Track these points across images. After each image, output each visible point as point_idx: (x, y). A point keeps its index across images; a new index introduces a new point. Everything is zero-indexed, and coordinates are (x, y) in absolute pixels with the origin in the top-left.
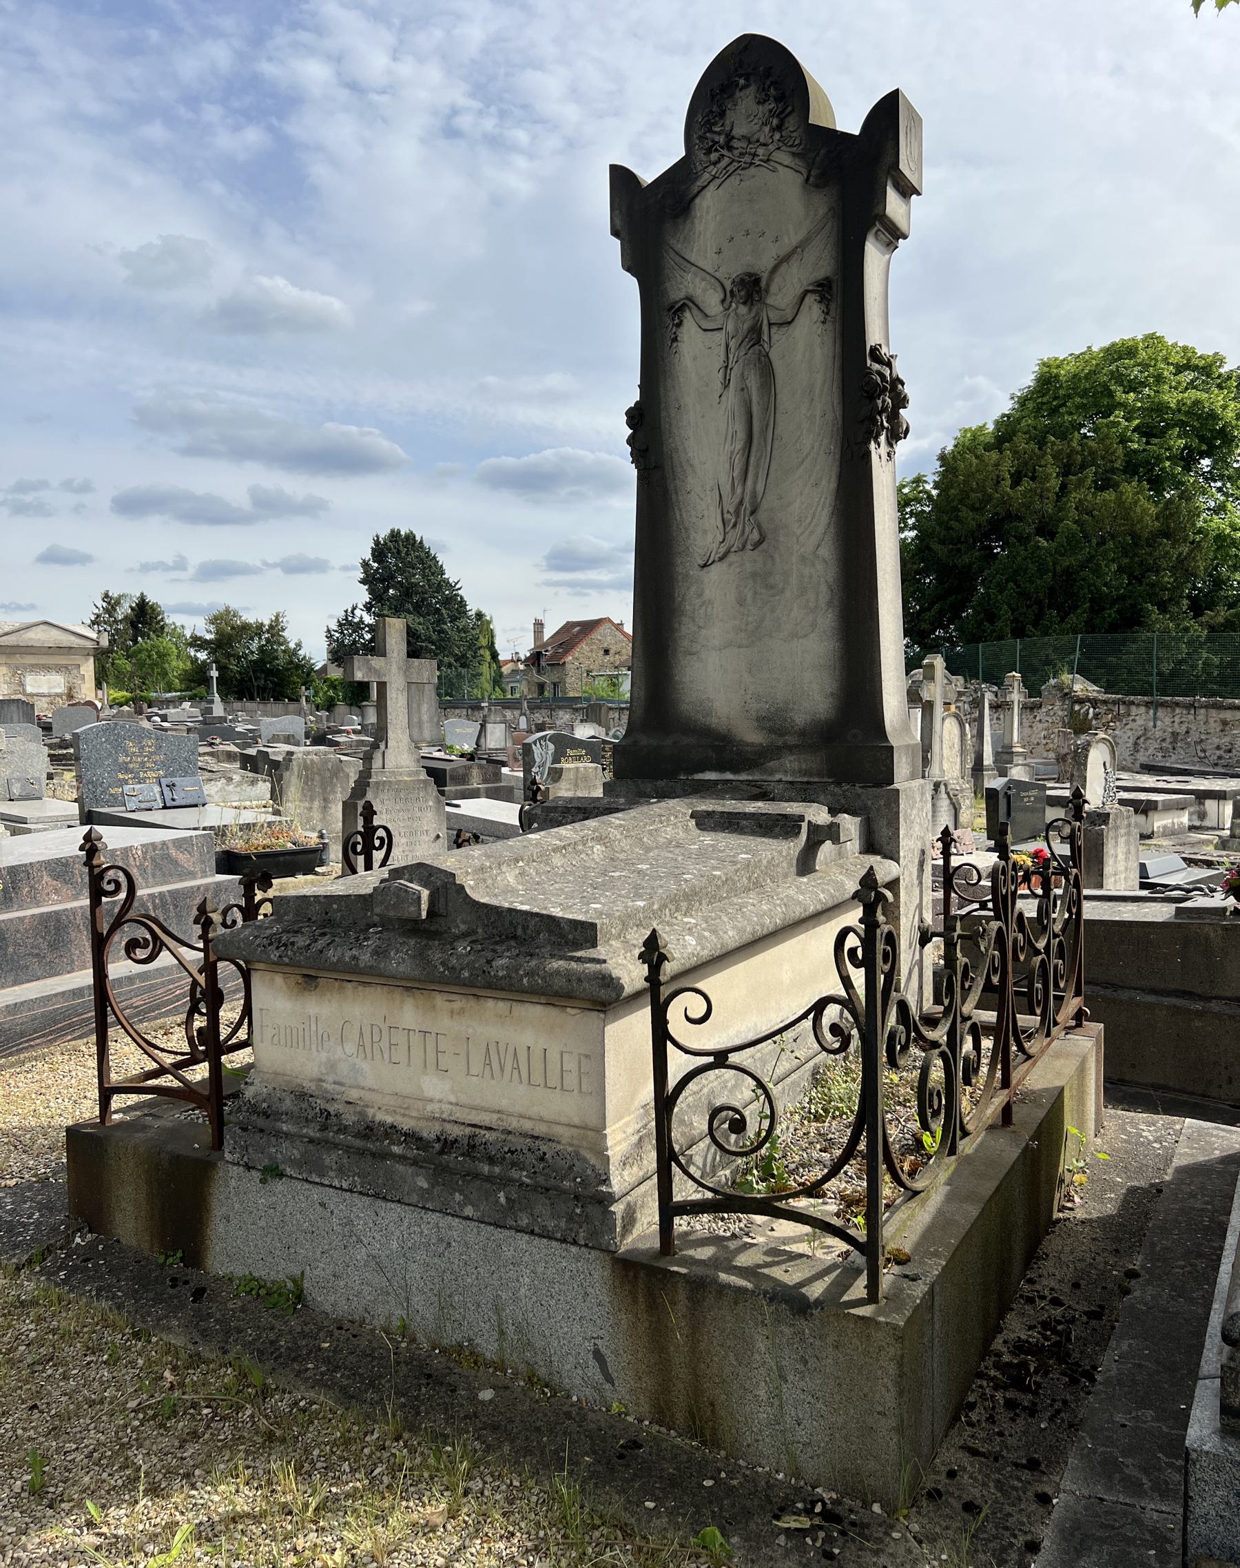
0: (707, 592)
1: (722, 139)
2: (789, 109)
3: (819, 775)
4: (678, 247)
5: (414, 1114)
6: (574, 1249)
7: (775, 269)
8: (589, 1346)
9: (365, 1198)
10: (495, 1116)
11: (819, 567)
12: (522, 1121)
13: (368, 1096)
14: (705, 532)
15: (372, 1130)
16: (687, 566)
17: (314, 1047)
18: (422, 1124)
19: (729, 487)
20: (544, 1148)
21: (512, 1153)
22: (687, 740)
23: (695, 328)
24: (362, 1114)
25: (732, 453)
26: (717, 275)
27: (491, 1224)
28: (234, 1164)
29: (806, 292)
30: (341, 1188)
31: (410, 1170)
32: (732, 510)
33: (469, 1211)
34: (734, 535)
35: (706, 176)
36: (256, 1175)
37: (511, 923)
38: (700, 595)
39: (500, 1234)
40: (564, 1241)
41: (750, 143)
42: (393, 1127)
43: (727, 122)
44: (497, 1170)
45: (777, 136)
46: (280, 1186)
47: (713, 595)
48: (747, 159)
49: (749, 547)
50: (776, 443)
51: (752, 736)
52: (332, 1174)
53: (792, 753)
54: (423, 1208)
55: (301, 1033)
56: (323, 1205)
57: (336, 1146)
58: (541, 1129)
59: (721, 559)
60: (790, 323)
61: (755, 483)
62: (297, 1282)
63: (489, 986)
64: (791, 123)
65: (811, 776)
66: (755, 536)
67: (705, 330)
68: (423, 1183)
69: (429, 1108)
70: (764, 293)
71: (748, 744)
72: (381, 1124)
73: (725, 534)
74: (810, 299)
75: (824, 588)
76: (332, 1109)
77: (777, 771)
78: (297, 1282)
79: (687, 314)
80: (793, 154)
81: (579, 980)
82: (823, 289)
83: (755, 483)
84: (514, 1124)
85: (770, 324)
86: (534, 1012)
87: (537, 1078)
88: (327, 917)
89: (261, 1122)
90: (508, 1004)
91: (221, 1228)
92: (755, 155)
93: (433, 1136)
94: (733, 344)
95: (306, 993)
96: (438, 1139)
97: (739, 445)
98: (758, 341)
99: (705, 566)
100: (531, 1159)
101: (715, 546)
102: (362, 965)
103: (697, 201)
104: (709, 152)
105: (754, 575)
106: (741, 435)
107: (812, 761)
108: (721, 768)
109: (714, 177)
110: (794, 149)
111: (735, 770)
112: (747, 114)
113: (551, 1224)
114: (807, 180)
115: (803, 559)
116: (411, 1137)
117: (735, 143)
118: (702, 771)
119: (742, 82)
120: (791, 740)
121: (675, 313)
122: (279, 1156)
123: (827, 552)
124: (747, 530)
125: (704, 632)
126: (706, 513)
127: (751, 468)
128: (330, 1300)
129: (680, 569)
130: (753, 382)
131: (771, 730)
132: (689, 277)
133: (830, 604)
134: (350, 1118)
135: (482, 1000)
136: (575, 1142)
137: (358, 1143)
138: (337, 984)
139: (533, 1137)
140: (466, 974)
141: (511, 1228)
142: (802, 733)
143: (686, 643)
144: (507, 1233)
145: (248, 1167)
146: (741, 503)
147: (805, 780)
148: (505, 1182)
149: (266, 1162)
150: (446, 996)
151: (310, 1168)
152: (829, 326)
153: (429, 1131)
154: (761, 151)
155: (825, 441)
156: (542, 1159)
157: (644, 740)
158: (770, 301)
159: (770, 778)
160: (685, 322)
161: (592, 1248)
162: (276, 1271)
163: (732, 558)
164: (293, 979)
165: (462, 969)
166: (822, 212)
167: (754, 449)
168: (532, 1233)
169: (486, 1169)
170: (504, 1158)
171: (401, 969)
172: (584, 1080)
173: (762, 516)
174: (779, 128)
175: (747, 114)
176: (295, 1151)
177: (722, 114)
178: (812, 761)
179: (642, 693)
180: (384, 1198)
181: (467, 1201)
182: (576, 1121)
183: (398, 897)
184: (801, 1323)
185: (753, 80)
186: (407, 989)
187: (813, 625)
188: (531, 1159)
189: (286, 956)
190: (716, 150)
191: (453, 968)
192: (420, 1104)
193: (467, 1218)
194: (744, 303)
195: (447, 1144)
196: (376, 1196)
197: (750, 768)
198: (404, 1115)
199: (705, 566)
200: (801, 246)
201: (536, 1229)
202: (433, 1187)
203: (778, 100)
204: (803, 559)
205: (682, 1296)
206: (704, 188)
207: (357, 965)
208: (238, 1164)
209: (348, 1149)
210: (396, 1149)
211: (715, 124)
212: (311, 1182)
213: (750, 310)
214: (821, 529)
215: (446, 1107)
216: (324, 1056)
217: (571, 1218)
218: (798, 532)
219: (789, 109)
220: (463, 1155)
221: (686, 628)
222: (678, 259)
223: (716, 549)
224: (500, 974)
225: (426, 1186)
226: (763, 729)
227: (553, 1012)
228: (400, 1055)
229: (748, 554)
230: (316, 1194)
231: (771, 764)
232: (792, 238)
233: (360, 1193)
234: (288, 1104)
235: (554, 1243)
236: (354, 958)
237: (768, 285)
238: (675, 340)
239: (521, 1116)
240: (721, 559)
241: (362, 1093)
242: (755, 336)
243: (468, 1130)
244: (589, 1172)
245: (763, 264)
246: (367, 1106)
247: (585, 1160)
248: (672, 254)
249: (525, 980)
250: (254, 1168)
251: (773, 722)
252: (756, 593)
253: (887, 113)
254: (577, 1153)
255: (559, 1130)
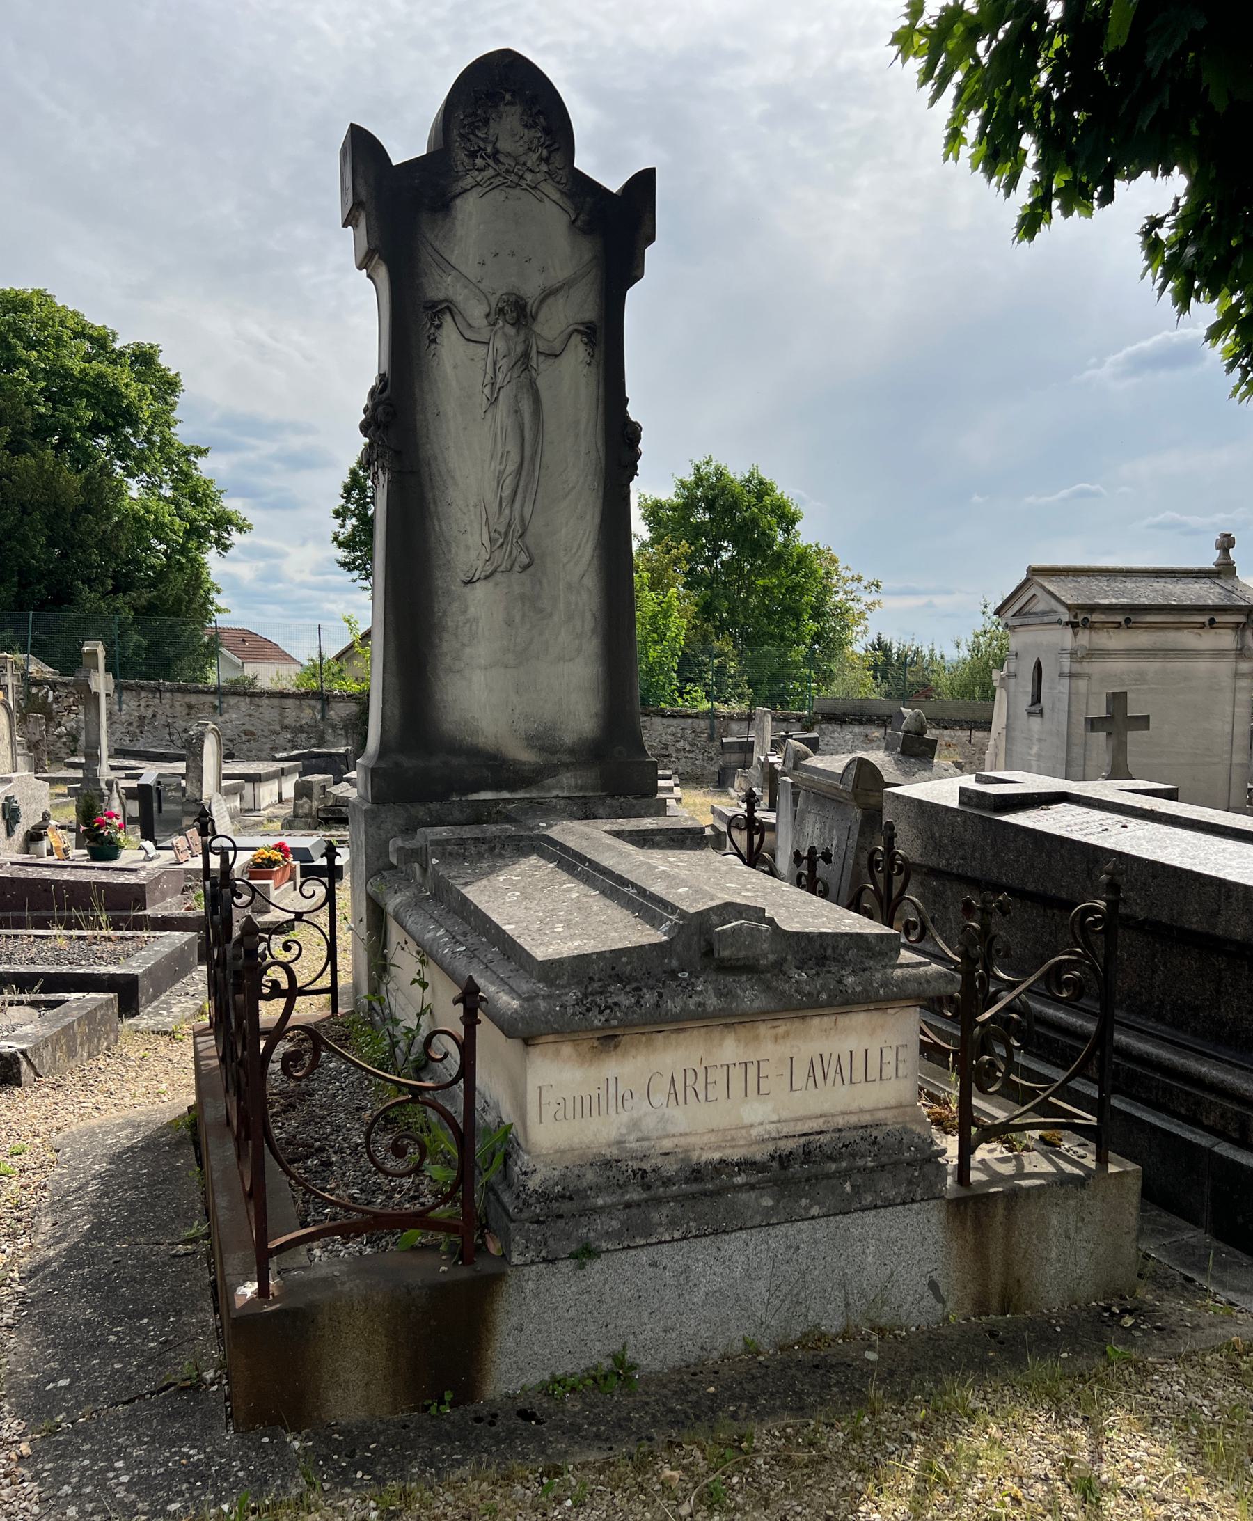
0: (472, 610)
1: (489, 149)
2: (556, 146)
3: (594, 789)
4: (437, 244)
5: (742, 1142)
6: (915, 1206)
7: (543, 301)
8: (925, 1281)
9: (703, 1240)
10: (821, 1121)
11: (585, 596)
12: (847, 1117)
13: (683, 1141)
14: (468, 548)
15: (699, 1172)
16: (448, 580)
17: (612, 1110)
18: (754, 1149)
19: (495, 506)
20: (875, 1133)
21: (847, 1146)
22: (456, 761)
23: (455, 335)
24: (686, 1160)
25: (501, 473)
26: (480, 285)
27: (836, 1215)
28: (526, 1265)
29: (576, 330)
30: (673, 1240)
31: (753, 1194)
32: (503, 531)
33: (815, 1211)
34: (498, 555)
35: (468, 181)
36: (567, 1266)
37: (821, 946)
38: (465, 612)
39: (846, 1220)
40: (904, 1203)
41: (517, 164)
42: (722, 1161)
43: (491, 131)
44: (844, 1164)
45: (544, 168)
46: (596, 1265)
47: (477, 617)
48: (512, 177)
49: (517, 568)
50: (543, 471)
51: (526, 756)
52: (660, 1230)
53: (568, 771)
54: (768, 1225)
55: (595, 1099)
56: (654, 1264)
57: (658, 1201)
58: (866, 1119)
59: (486, 578)
60: (556, 356)
61: (522, 506)
62: (618, 1359)
63: (847, 1003)
64: (557, 159)
65: (586, 790)
66: (524, 559)
67: (468, 340)
68: (767, 1202)
69: (754, 1132)
70: (530, 320)
71: (524, 763)
72: (709, 1163)
73: (492, 552)
74: (576, 339)
75: (588, 616)
76: (647, 1166)
77: (554, 788)
78: (618, 1359)
79: (448, 318)
80: (562, 192)
81: (928, 982)
82: (589, 332)
83: (522, 506)
84: (841, 1122)
85: (538, 352)
86: (859, 1019)
87: (859, 1075)
88: (613, 973)
89: (565, 1207)
90: (833, 1018)
91: (510, 1343)
92: (522, 177)
93: (766, 1157)
94: (504, 364)
95: (603, 1055)
96: (773, 1157)
97: (512, 467)
98: (527, 367)
99: (469, 582)
100: (865, 1146)
101: (480, 564)
102: (710, 1009)
103: (458, 201)
104: (473, 155)
105: (523, 598)
106: (514, 457)
107: (588, 777)
108: (497, 787)
109: (478, 184)
110: (561, 187)
111: (512, 789)
112: (509, 129)
113: (891, 1194)
114: (574, 222)
115: (569, 587)
116: (746, 1165)
117: (502, 158)
118: (477, 791)
119: (508, 97)
120: (566, 758)
121: (435, 314)
122: (592, 1234)
123: (591, 582)
124: (515, 552)
125: (468, 650)
126: (468, 529)
127: (520, 490)
128: (651, 1359)
129: (439, 583)
130: (526, 407)
131: (542, 749)
132: (449, 279)
133: (594, 631)
134: (670, 1168)
135: (808, 1020)
136: (900, 1120)
137: (695, 1188)
138: (644, 1038)
139: (862, 1127)
140: (825, 997)
141: (856, 1211)
142: (572, 751)
143: (448, 660)
144: (856, 1215)
145: (550, 1261)
146: (509, 526)
147: (581, 794)
148: (845, 1174)
149: (574, 1247)
150: (770, 1024)
151: (635, 1231)
152: (593, 369)
153: (760, 1153)
154: (529, 176)
155: (589, 478)
156: (874, 1143)
157: (406, 762)
158: (536, 328)
159: (548, 795)
160: (445, 325)
161: (928, 1199)
162: (597, 1354)
163: (498, 577)
164: (585, 1046)
165: (819, 993)
166: (587, 257)
167: (524, 473)
168: (875, 1207)
169: (833, 1167)
170: (841, 1154)
171: (757, 1004)
172: (900, 1066)
173: (529, 539)
174: (547, 160)
175: (509, 129)
176: (614, 1223)
177: (486, 122)
178: (588, 777)
179: (396, 712)
180: (724, 1232)
181: (814, 1201)
182: (893, 1103)
183: (752, 936)
184: (1084, 1194)
185: (505, 99)
186: (726, 1025)
187: (579, 650)
188: (865, 1146)
189: (616, 1018)
190: (481, 156)
191: (809, 993)
192: (743, 1132)
193: (813, 1218)
194: (512, 325)
195: (784, 1160)
196: (715, 1233)
197: (527, 786)
198: (733, 1147)
199: (469, 582)
200: (567, 285)
201: (879, 1203)
202: (778, 1202)
203: (547, 131)
204: (569, 587)
205: (1000, 1209)
206: (466, 191)
207: (704, 1010)
208: (533, 1262)
209: (675, 1198)
210: (739, 1180)
211: (478, 128)
212: (636, 1247)
213: (518, 332)
214: (585, 560)
215: (770, 1127)
216: (625, 1117)
217: (910, 1182)
218: (565, 560)
219: (556, 146)
220: (804, 1163)
221: (447, 645)
222: (436, 257)
223: (481, 569)
224: (858, 990)
225: (770, 1203)
226: (533, 747)
227: (876, 1015)
228: (718, 1091)
229: (515, 576)
230: (644, 1256)
231: (549, 781)
232: (560, 273)
233: (696, 1237)
234: (590, 1177)
235: (900, 1208)
236: (699, 1004)
237: (537, 313)
238: (434, 341)
239: (843, 1113)
240: (486, 578)
241: (676, 1140)
242: (524, 361)
243: (802, 1140)
244: (916, 1140)
245: (530, 290)
246: (687, 1151)
247: (913, 1132)
248: (430, 249)
249: (881, 992)
250: (556, 1259)
251: (542, 741)
252: (524, 616)
253: (644, 182)
254: (904, 1128)
255: (881, 1115)
